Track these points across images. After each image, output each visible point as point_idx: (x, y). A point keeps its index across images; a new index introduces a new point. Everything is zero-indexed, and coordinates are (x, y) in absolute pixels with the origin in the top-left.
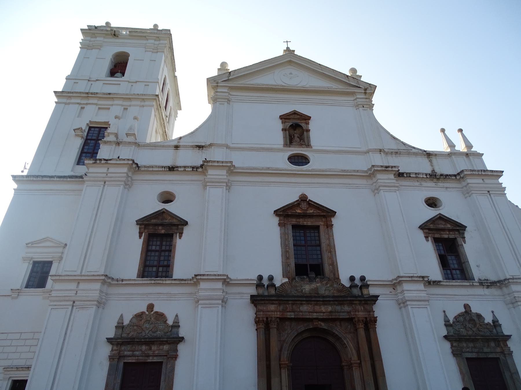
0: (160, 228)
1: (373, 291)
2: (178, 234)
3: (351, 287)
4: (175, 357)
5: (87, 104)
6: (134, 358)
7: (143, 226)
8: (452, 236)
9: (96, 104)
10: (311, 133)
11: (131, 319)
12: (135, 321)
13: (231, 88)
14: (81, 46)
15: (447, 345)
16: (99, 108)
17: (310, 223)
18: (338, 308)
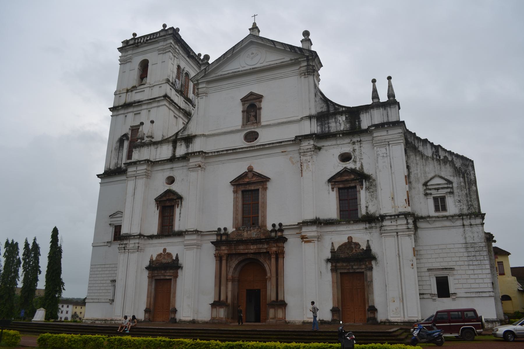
0: (168, 202)
1: (286, 233)
2: (177, 205)
3: (272, 231)
4: (176, 276)
5: (127, 113)
6: (159, 277)
7: (158, 202)
8: (352, 185)
9: (133, 112)
11: (156, 257)
12: (158, 258)
13: (208, 82)
14: (120, 63)
15: (330, 265)
16: (135, 114)
17: (253, 188)
18: (261, 246)
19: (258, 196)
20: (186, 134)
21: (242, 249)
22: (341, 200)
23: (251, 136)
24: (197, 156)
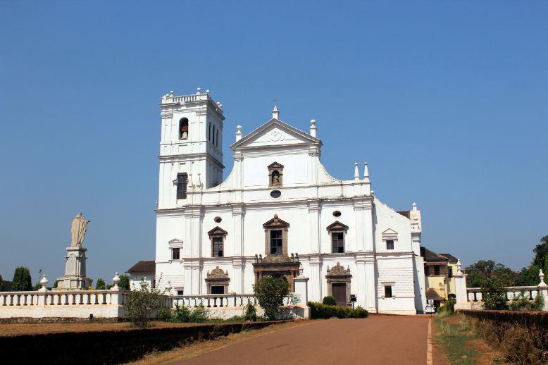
10: (283, 176)
13: (242, 150)
22: (334, 241)
23: (276, 194)
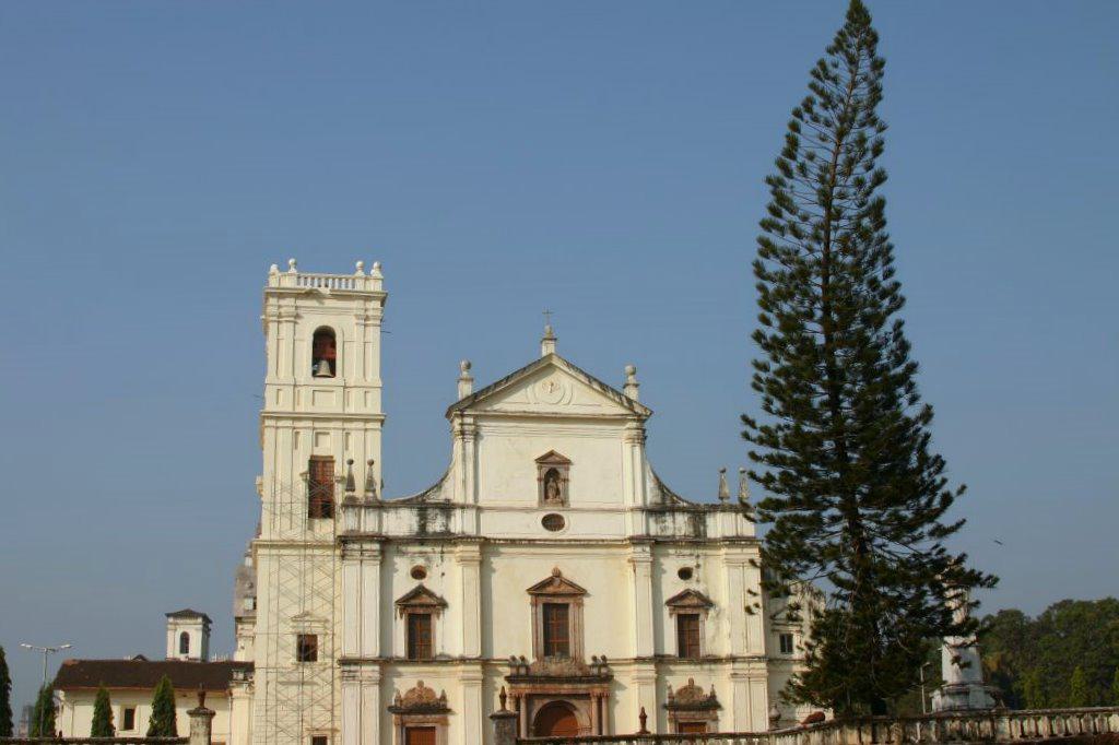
3: (593, 666)
4: (445, 724)
8: (695, 612)
18: (579, 686)
19: (567, 614)
20: (441, 497)
21: (551, 688)
23: (553, 522)
24: (473, 543)
